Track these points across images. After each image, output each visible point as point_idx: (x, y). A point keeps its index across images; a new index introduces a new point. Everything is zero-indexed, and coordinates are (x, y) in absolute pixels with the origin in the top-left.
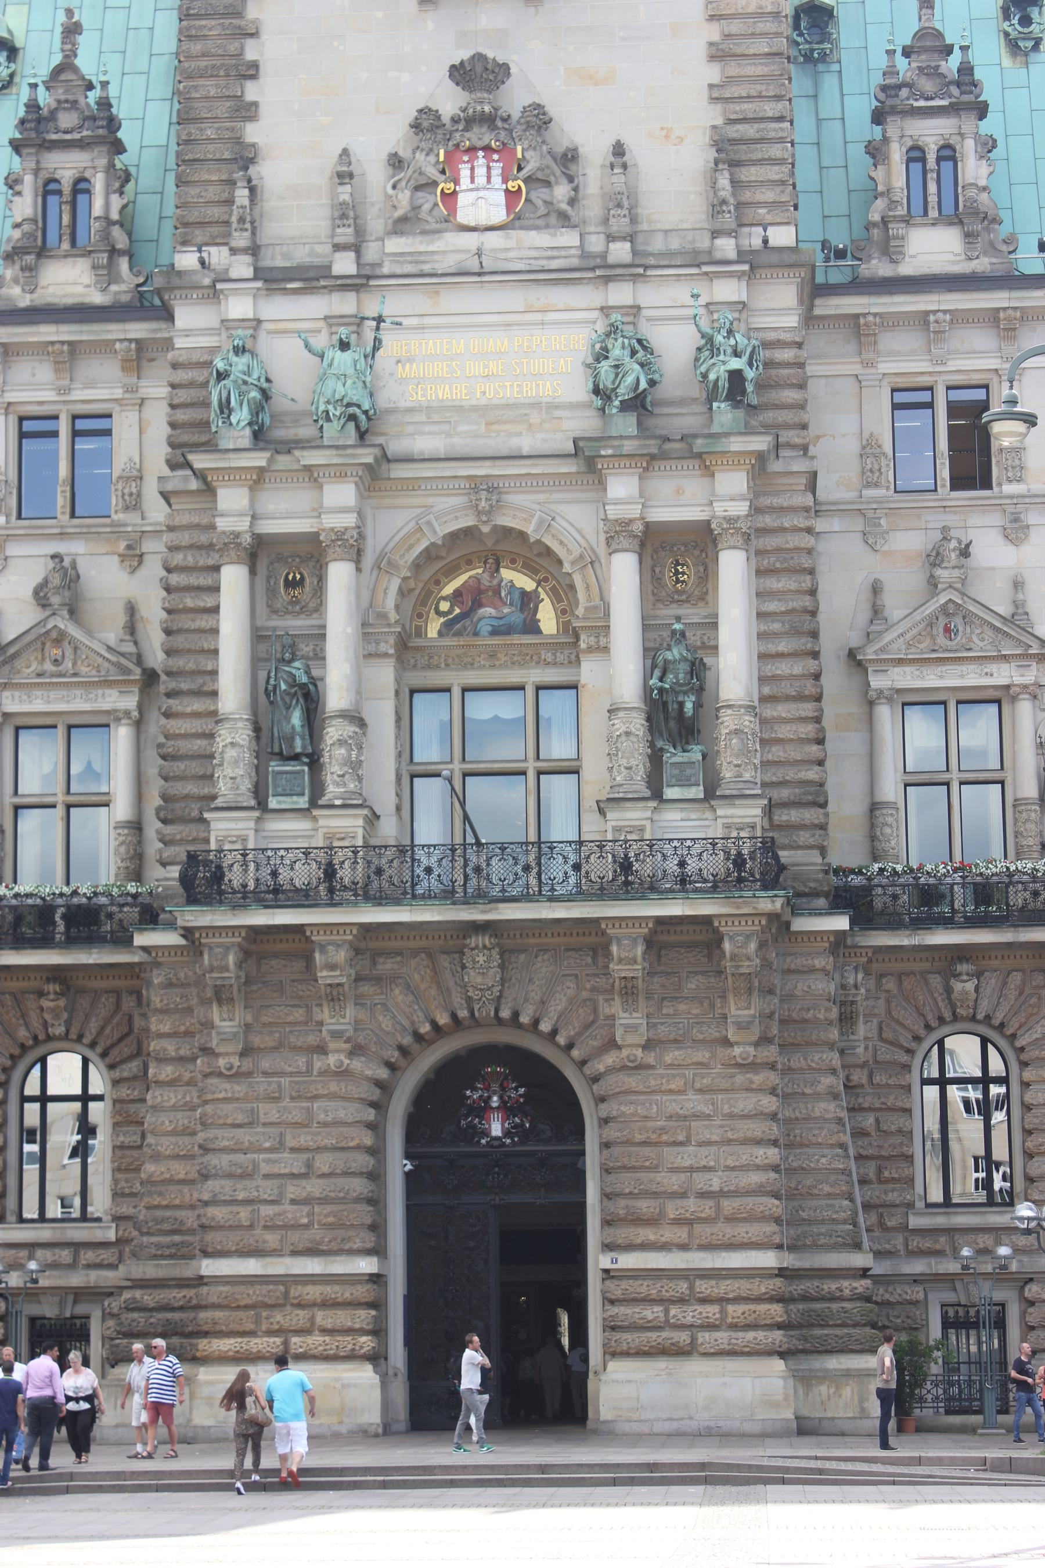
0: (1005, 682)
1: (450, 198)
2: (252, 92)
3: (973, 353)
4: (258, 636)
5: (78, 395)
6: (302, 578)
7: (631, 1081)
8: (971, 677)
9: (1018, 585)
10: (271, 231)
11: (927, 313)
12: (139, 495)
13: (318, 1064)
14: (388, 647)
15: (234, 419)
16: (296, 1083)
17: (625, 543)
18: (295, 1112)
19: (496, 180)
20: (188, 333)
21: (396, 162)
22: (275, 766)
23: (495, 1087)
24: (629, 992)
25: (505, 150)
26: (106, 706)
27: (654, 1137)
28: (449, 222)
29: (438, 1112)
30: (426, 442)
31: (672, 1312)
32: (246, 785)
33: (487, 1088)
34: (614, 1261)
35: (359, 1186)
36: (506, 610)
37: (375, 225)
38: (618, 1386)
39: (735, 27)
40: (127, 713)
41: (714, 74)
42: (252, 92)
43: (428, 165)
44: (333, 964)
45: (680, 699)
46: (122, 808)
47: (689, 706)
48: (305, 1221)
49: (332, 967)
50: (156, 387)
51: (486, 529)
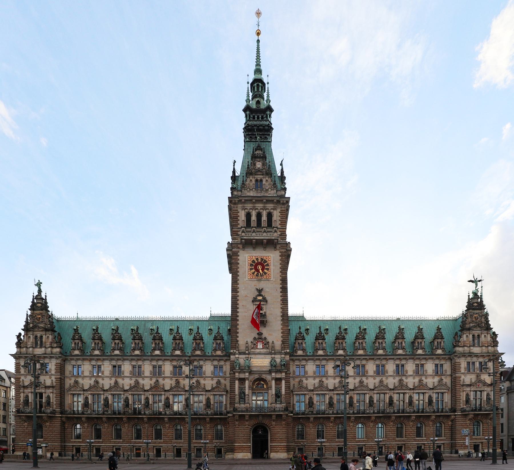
2: (238, 335)
4: (239, 387)
10: (240, 348)
18: (243, 431)
21: (252, 342)
24: (274, 421)
25: (262, 342)
29: (255, 431)
30: (254, 369)
37: (250, 348)
38: (273, 455)
41: (282, 335)
42: (238, 335)
43: (255, 342)
44: (247, 418)
50: (228, 363)
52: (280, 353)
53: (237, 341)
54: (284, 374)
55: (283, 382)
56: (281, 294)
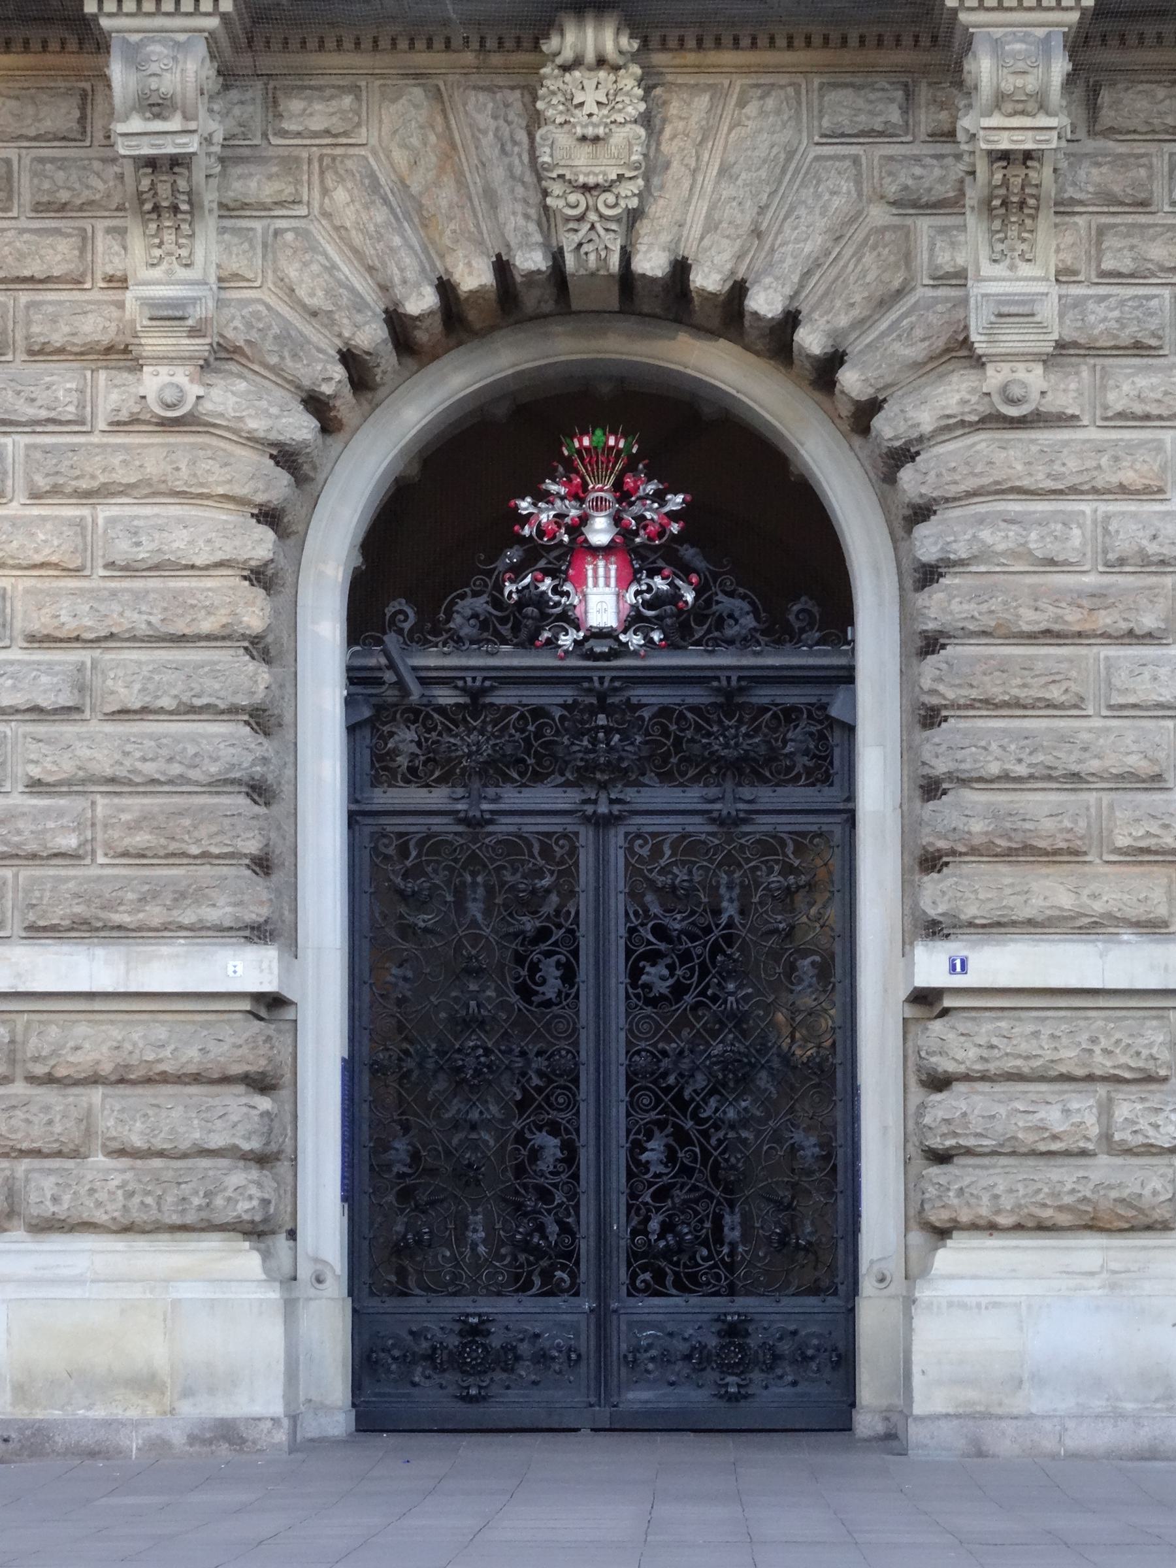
7: (1008, 456)
13: (112, 393)
16: (47, 450)
23: (601, 489)
27: (1073, 619)
31: (1123, 1111)
33: (578, 496)
34: (959, 966)
35: (227, 744)
48: (70, 842)
49: (156, 106)
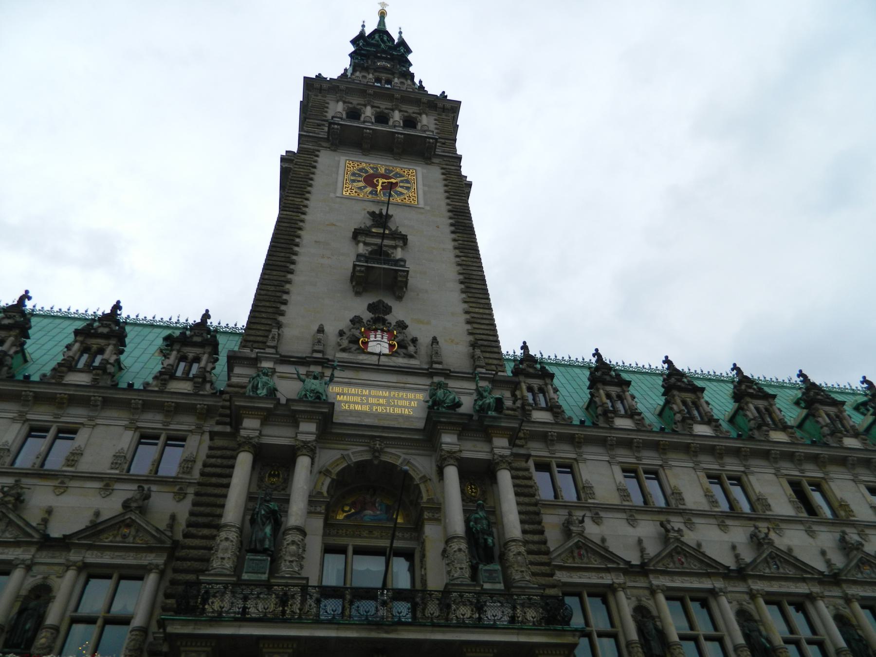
0: (610, 582)
1: (366, 344)
3: (564, 451)
4: (250, 497)
5: (172, 427)
6: (279, 474)
8: (593, 579)
9: (603, 540)
11: (548, 432)
12: (191, 468)
14: (322, 509)
15: (259, 392)
17: (452, 462)
19: (386, 340)
20: (239, 376)
21: (341, 333)
22: (249, 556)
25: (388, 332)
26: (146, 562)
28: (363, 351)
32: (228, 564)
36: (378, 512)
39: (476, 315)
40: (157, 566)
42: (283, 308)
43: (357, 333)
45: (486, 537)
46: (138, 621)
47: (490, 541)
51: (376, 462)
52: (472, 377)
53: (279, 326)
54: (501, 444)
55: (505, 478)
56: (453, 236)
